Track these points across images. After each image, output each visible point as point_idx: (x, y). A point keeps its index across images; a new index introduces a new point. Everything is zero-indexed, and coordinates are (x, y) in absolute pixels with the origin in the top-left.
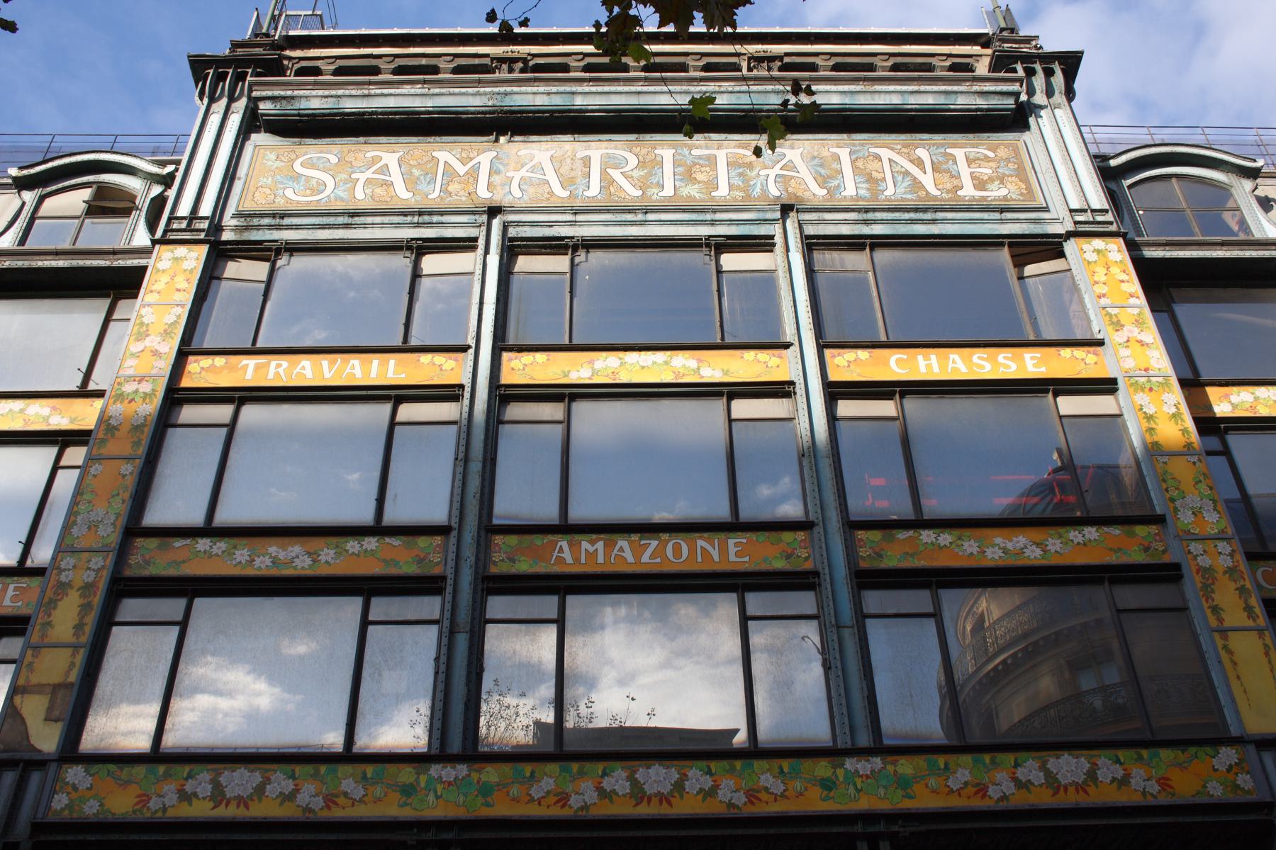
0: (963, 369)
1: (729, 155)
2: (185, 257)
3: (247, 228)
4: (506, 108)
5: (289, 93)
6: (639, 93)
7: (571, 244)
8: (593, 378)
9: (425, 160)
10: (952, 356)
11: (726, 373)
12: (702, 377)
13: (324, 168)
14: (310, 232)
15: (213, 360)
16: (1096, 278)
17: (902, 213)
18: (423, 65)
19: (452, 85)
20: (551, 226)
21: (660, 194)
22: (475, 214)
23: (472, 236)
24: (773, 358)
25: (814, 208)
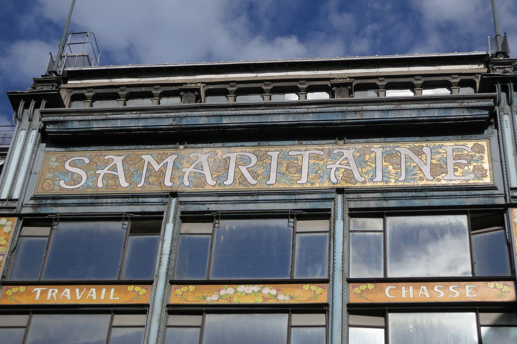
0: (428, 296)
2: (5, 225)
3: (39, 206)
4: (183, 126)
5: (62, 118)
6: (259, 115)
7: (215, 215)
8: (219, 300)
9: (137, 161)
10: (422, 287)
11: (292, 298)
12: (278, 300)
13: (81, 167)
14: (73, 208)
15: (19, 288)
17: (407, 192)
18: (143, 91)
19: (153, 112)
20: (205, 204)
21: (267, 183)
22: (162, 197)
23: (161, 210)
24: (319, 289)
25: (356, 191)
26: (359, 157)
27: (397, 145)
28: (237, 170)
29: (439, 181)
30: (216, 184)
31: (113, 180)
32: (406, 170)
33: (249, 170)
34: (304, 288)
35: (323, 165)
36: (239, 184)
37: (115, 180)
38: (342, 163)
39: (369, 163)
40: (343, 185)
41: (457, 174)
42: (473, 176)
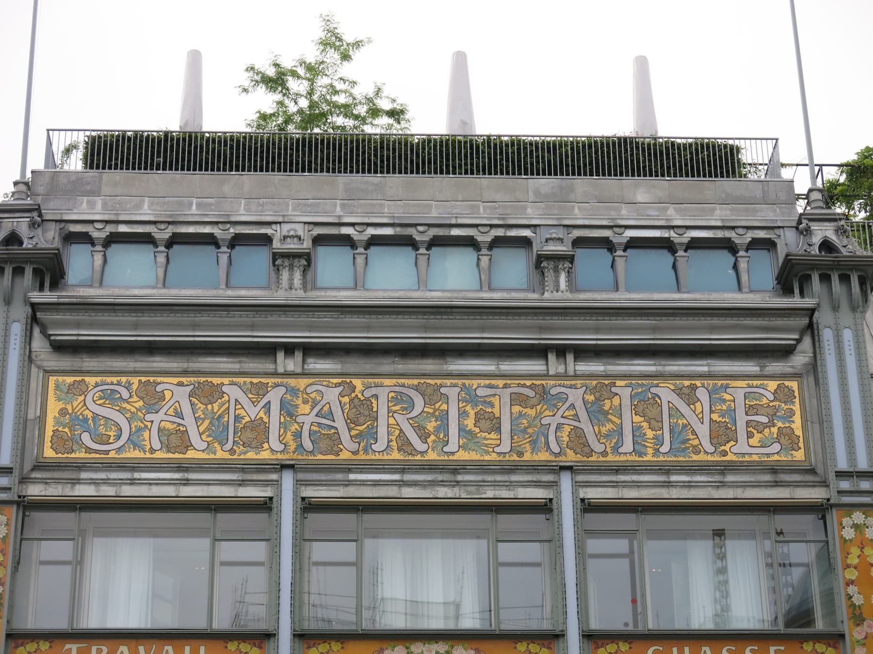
1: (513, 395)
15: (38, 643)
16: (849, 562)
21: (445, 449)
26: (593, 403)
27: (655, 382)
28: (391, 421)
29: (724, 456)
30: (358, 450)
31: (178, 435)
32: (671, 431)
33: (411, 422)
34: (518, 648)
35: (534, 417)
36: (398, 449)
37: (181, 435)
38: (564, 415)
39: (610, 416)
40: (571, 457)
41: (754, 441)
42: (776, 447)
